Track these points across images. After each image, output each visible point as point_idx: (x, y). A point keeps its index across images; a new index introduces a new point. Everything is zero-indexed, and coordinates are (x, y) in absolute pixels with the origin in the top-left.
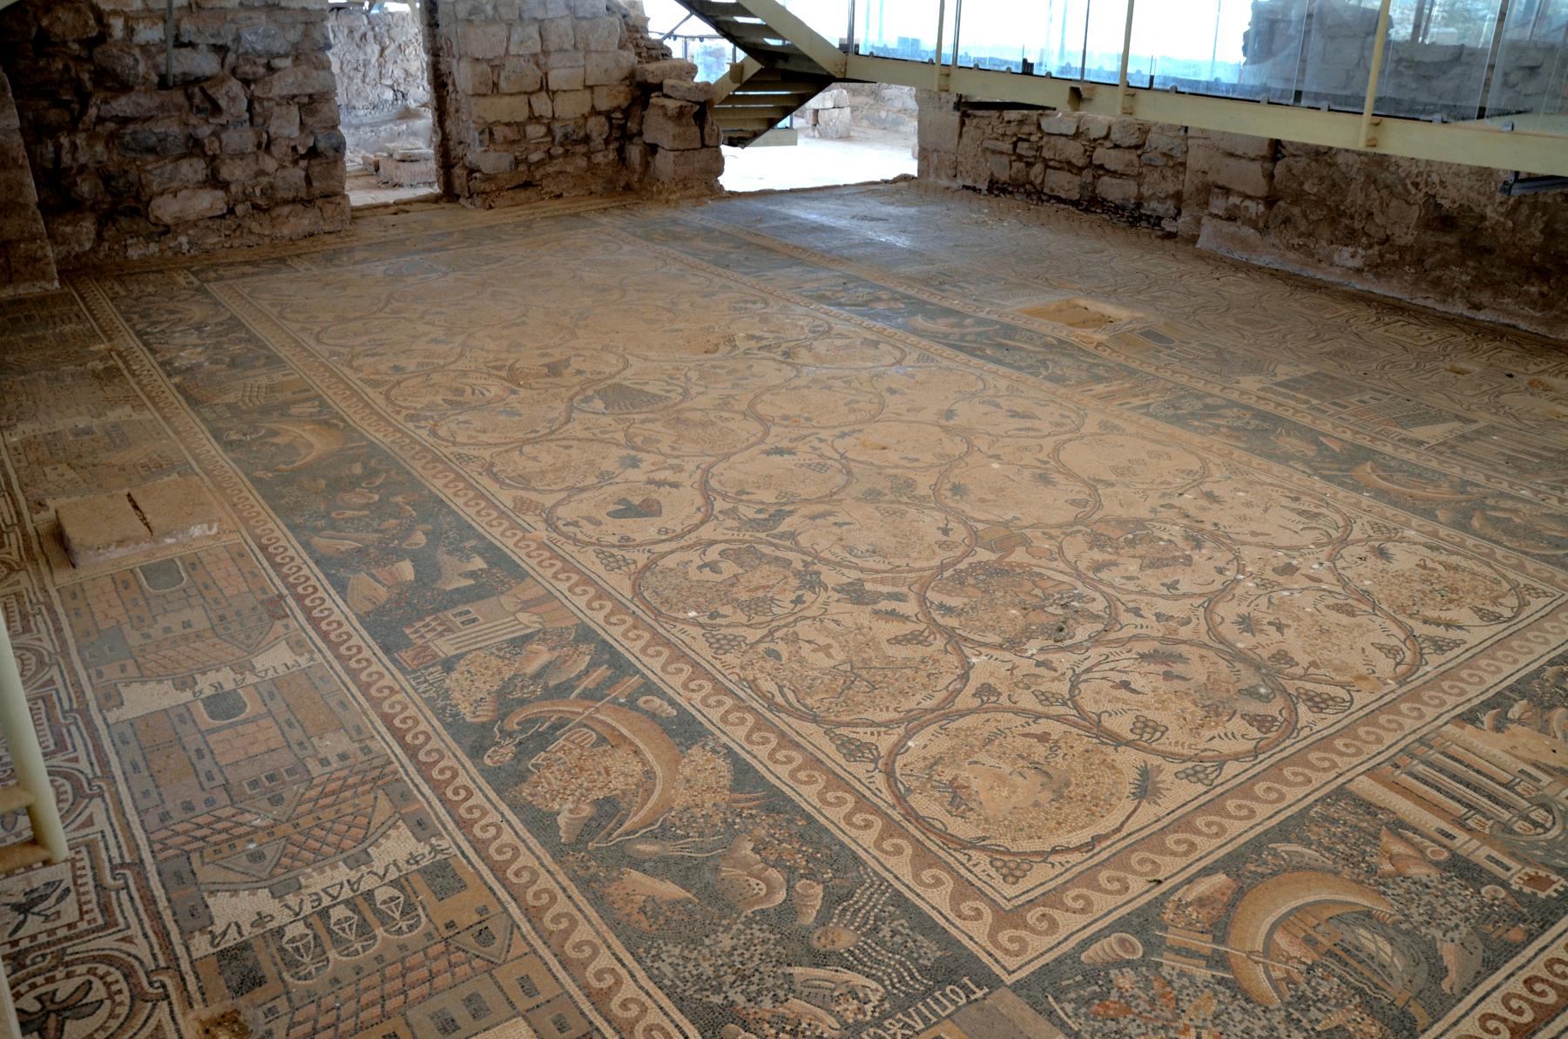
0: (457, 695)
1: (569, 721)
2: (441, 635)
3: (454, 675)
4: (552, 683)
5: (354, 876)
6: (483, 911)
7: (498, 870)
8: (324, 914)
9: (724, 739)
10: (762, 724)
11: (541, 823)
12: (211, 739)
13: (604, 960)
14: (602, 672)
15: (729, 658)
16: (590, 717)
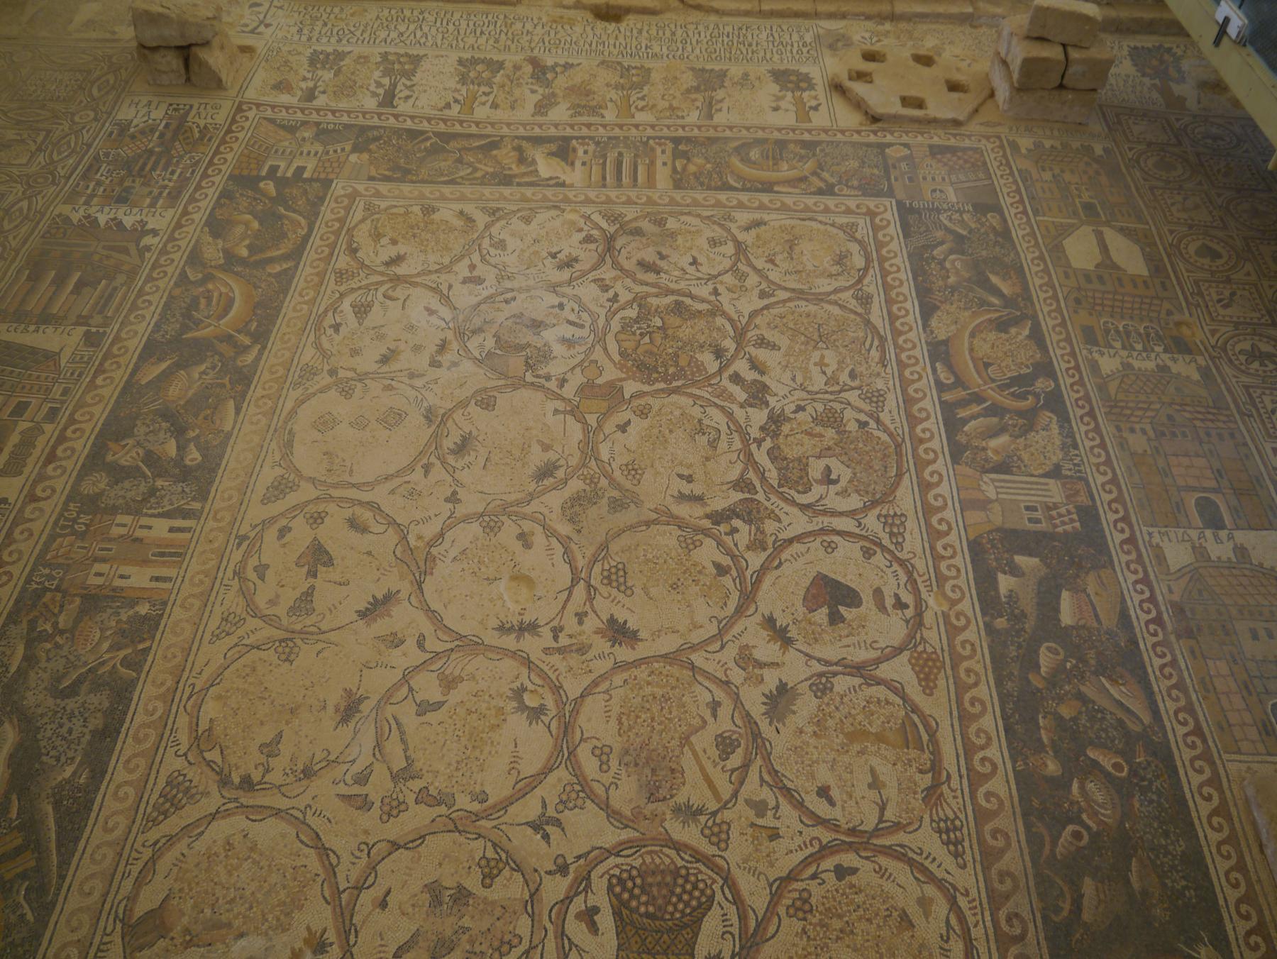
0: (1058, 443)
1: (999, 387)
2: (1055, 506)
3: (1055, 459)
4: (995, 420)
5: (1130, 360)
6: (1076, 312)
7: (1063, 324)
8: (1145, 350)
9: (923, 336)
10: (897, 333)
11: (1037, 336)
12: (1213, 484)
13: (1034, 269)
14: (962, 413)
15: (880, 384)
16: (985, 383)
